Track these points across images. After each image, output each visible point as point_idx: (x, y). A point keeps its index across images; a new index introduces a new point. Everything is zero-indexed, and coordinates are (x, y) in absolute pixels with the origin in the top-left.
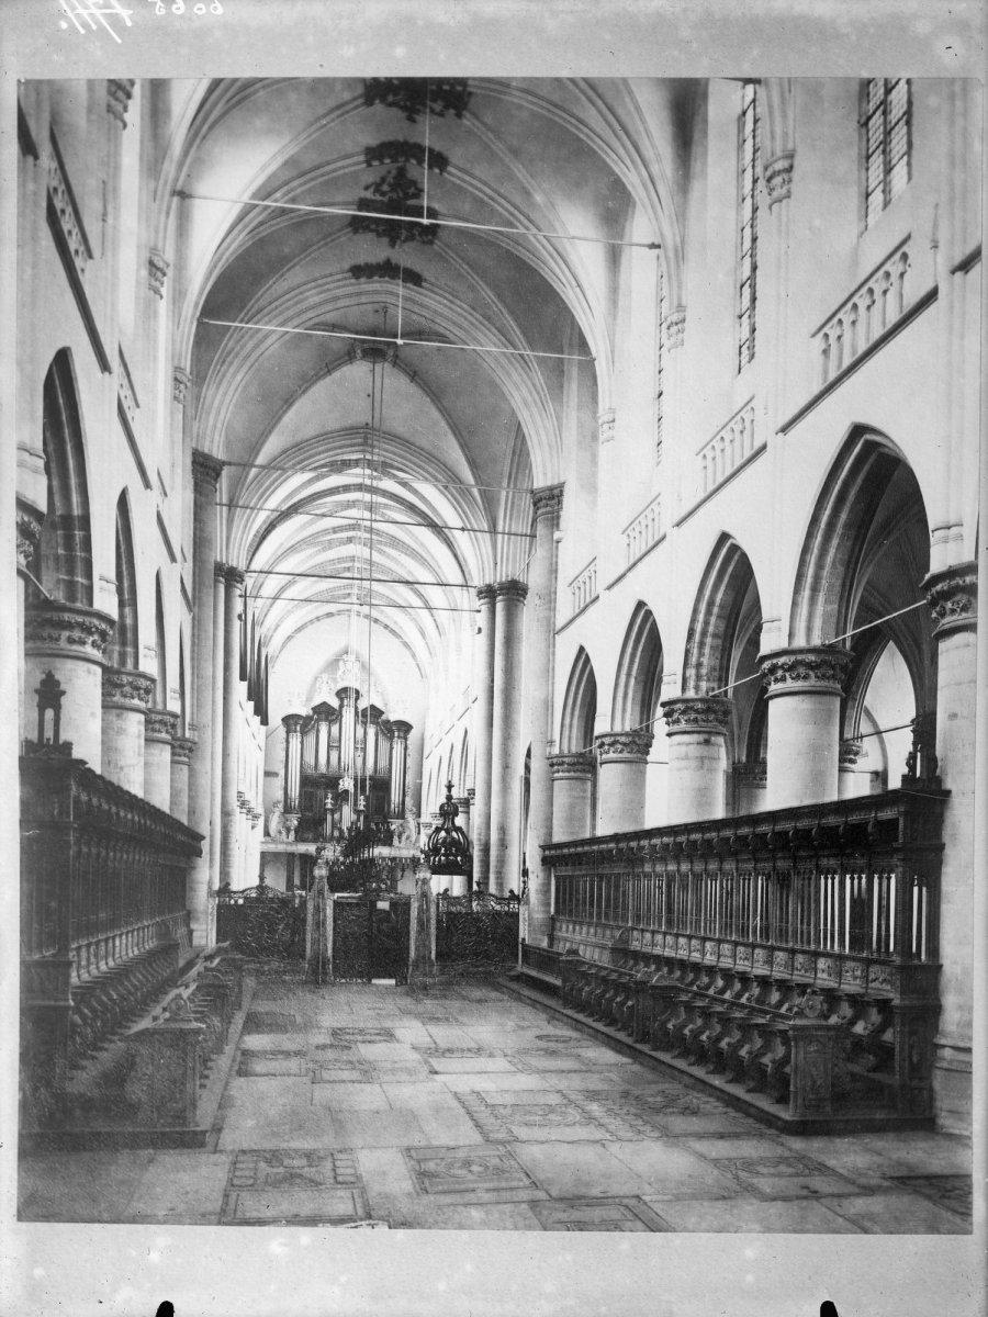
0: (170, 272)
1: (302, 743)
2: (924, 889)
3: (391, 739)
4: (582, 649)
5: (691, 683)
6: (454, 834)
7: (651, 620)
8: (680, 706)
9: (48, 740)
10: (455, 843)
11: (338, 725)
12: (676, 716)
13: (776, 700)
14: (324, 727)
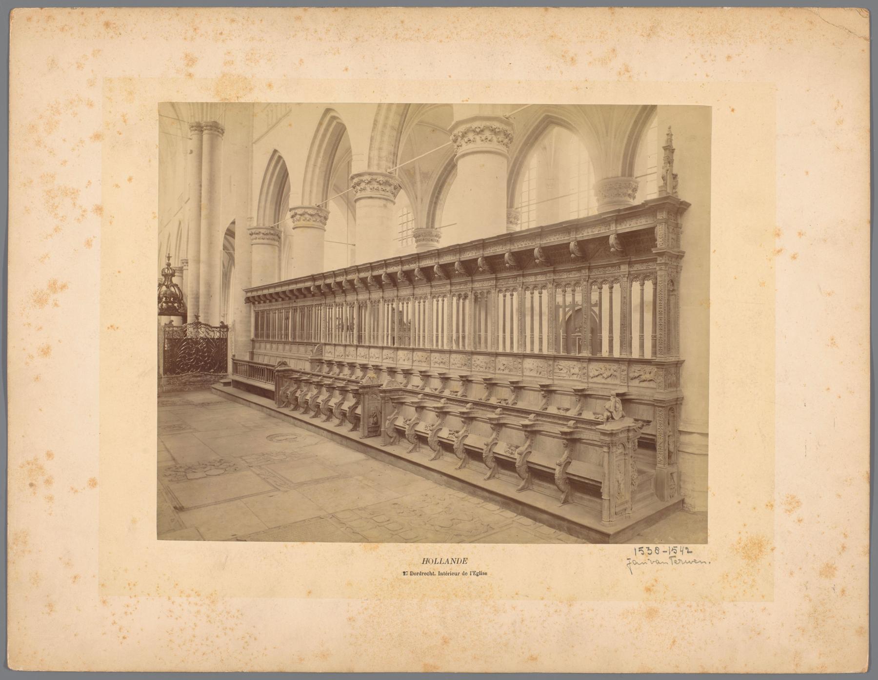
6: (172, 289)
8: (367, 178)
10: (173, 295)
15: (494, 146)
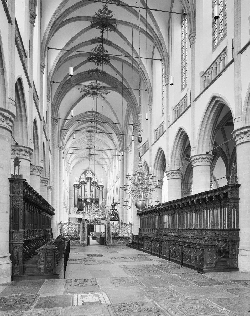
0: (46, 67)
1: (78, 191)
2: (235, 210)
3: (99, 189)
4: (145, 162)
5: (173, 166)
6: (115, 211)
7: (162, 153)
9: (17, 174)
12: (169, 175)
13: (195, 167)
14: (83, 187)
15: (204, 163)
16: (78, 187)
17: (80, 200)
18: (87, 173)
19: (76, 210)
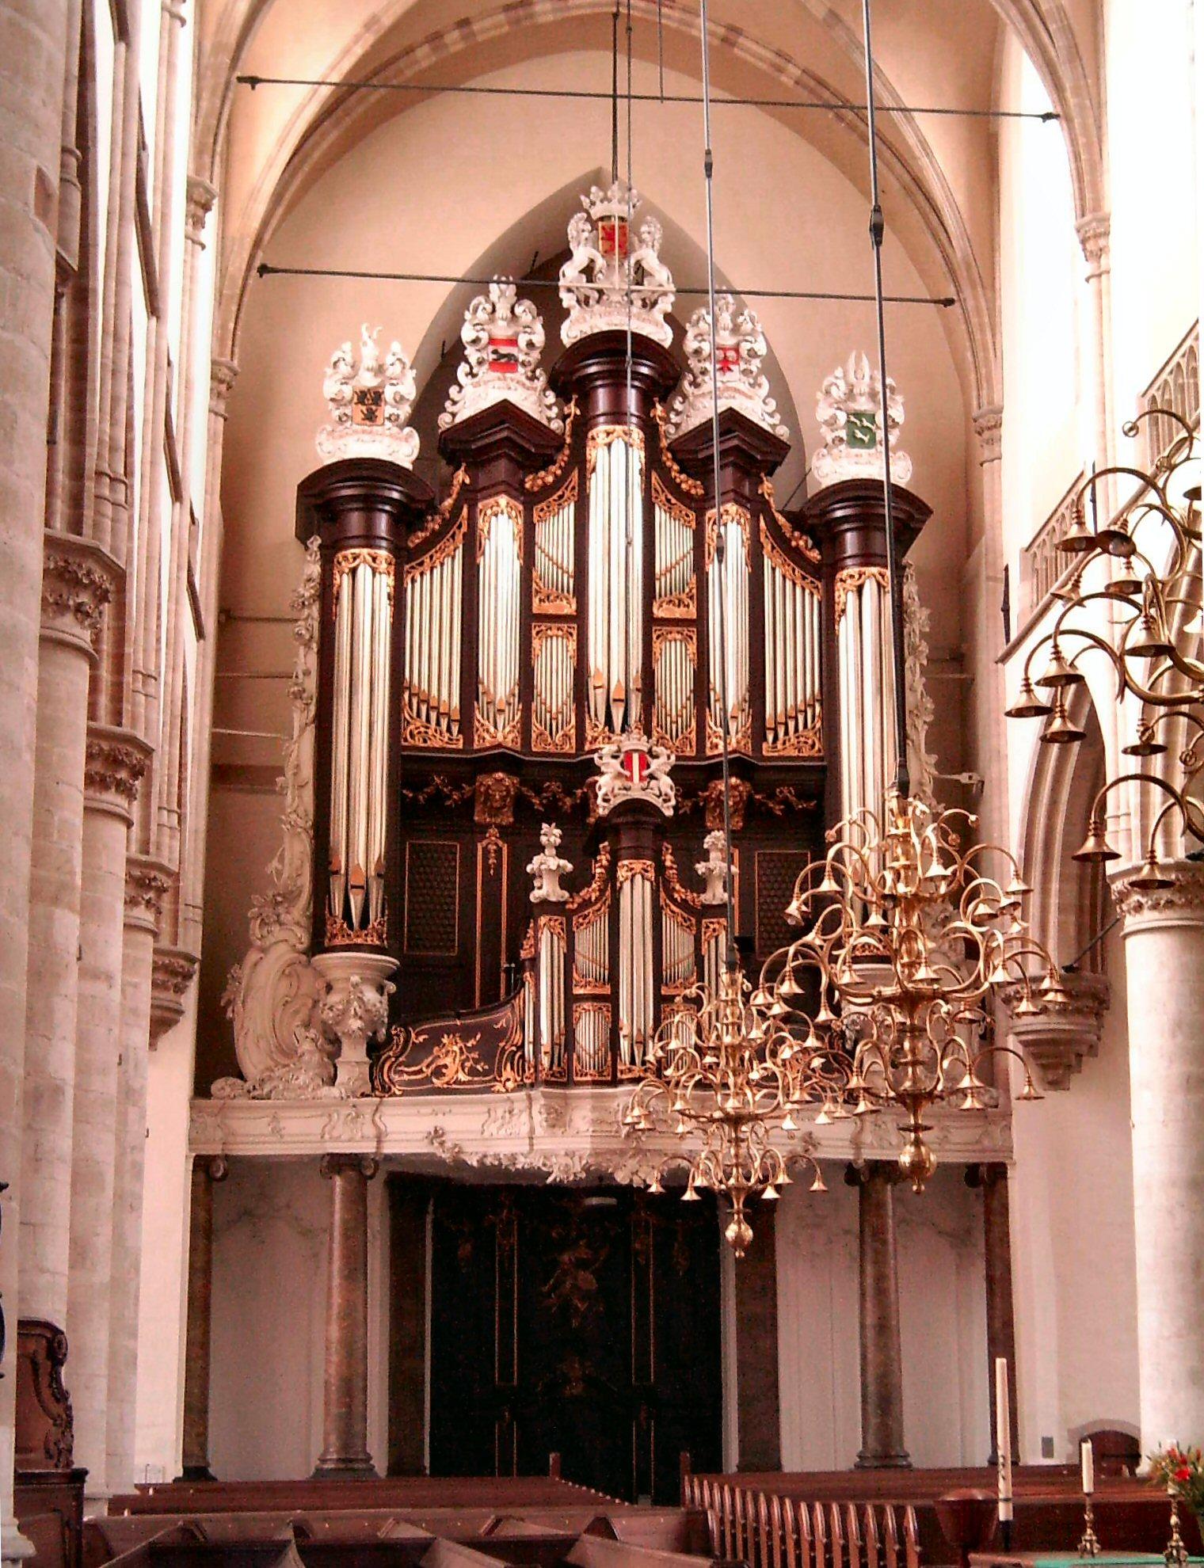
1: (398, 599)
3: (824, 575)
11: (569, 512)
16: (407, 518)
17: (433, 790)
18: (581, 255)
19: (357, 986)
